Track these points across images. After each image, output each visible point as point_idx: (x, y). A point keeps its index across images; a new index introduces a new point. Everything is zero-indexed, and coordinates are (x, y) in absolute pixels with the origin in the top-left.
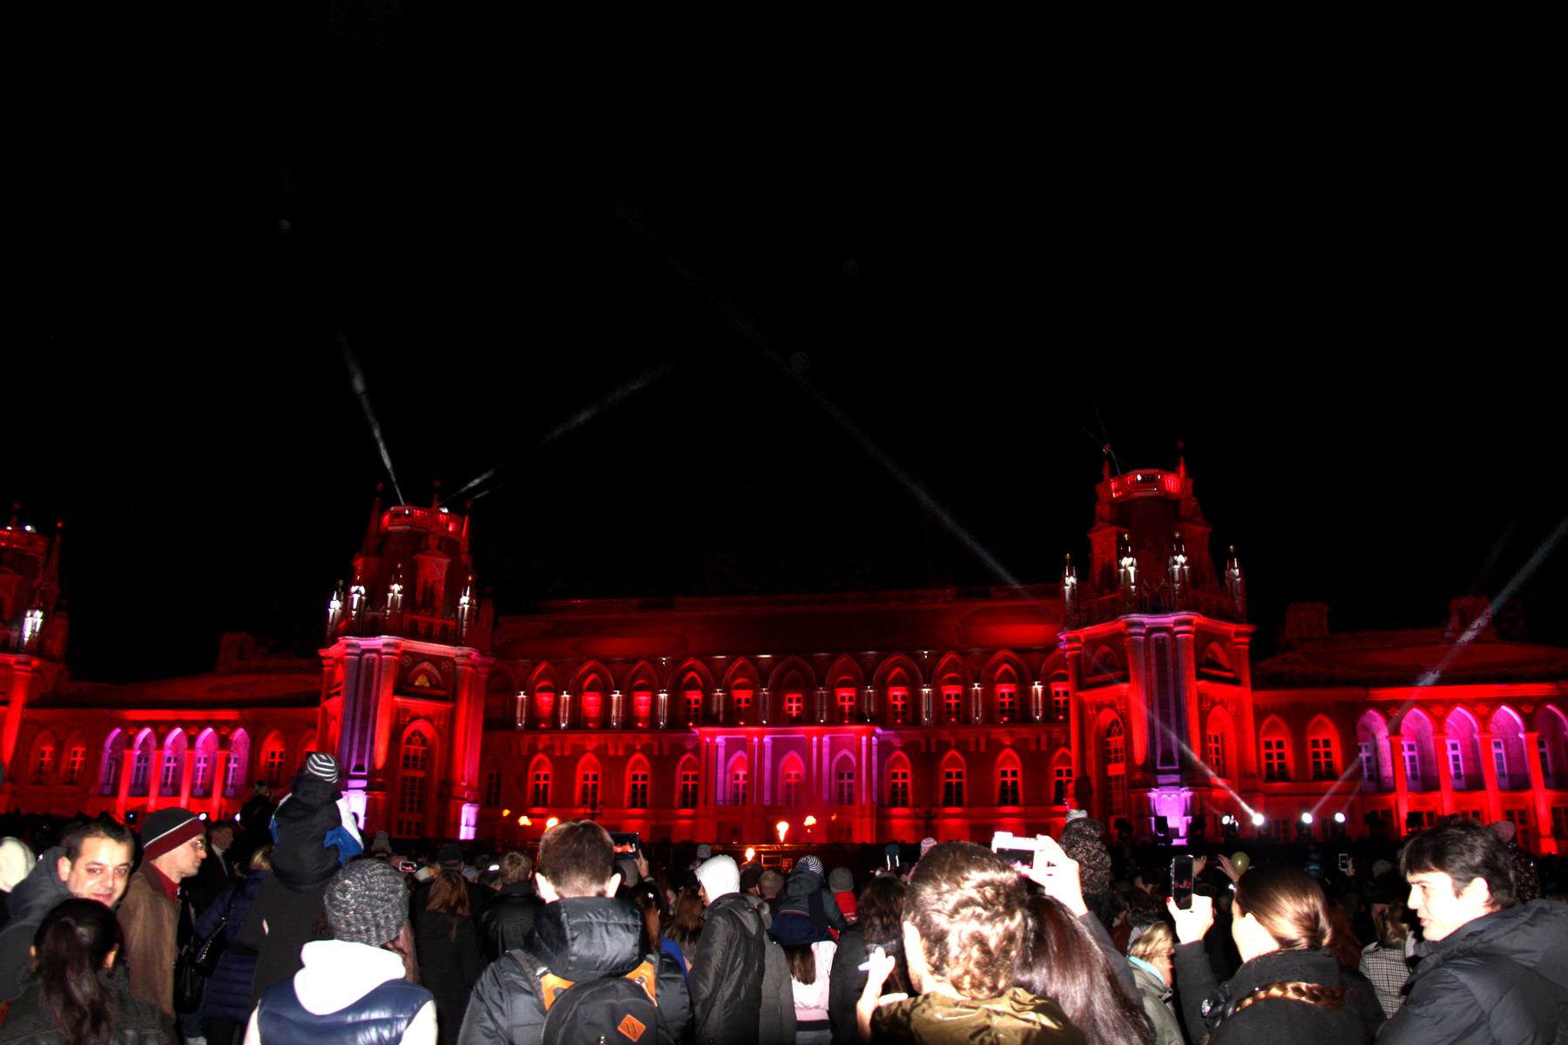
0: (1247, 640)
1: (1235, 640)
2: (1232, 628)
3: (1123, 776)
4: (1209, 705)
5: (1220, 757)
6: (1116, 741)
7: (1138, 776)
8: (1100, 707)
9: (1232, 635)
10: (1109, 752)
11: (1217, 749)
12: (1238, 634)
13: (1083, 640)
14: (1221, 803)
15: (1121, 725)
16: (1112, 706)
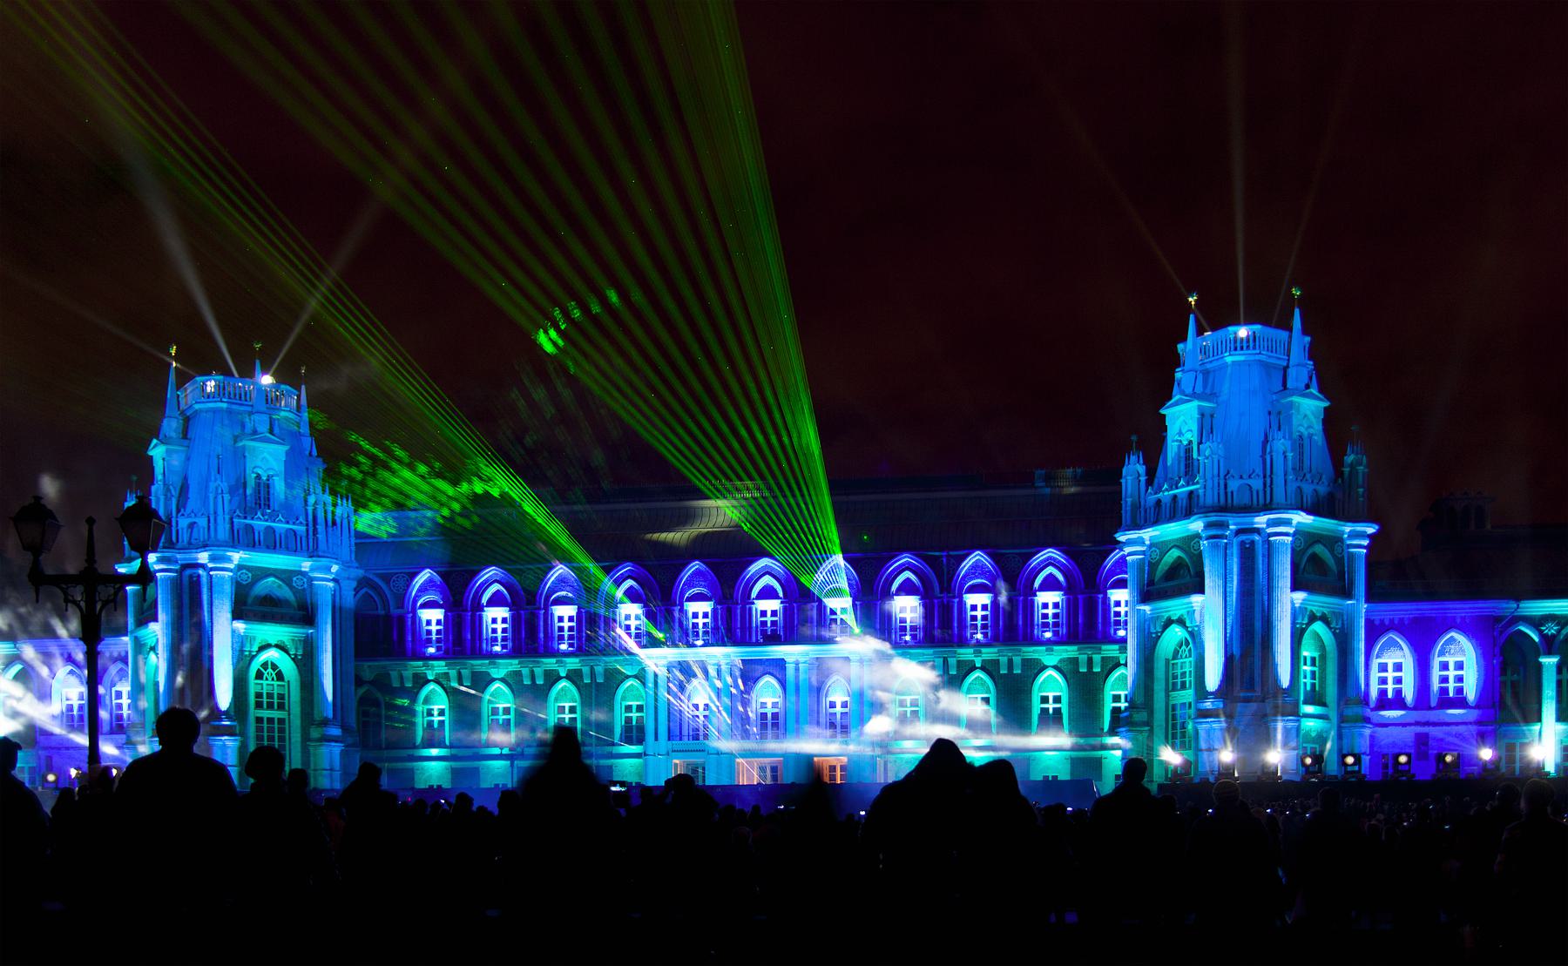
0: (1365, 542)
1: (1349, 542)
2: (1347, 528)
3: (1190, 704)
4: (1306, 621)
5: (1317, 682)
6: (1187, 664)
7: (1208, 705)
8: (1169, 622)
9: (1346, 536)
10: (1175, 677)
11: (1313, 673)
12: (1353, 535)
13: (1147, 543)
14: (1313, 734)
15: (1191, 645)
16: (1181, 622)
